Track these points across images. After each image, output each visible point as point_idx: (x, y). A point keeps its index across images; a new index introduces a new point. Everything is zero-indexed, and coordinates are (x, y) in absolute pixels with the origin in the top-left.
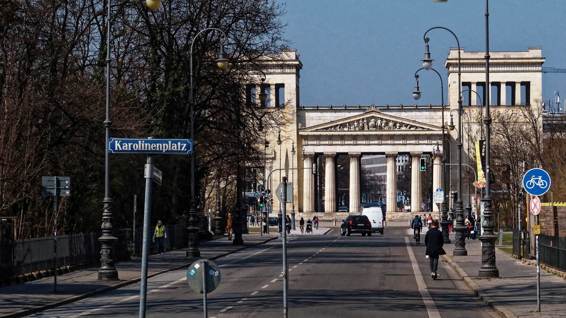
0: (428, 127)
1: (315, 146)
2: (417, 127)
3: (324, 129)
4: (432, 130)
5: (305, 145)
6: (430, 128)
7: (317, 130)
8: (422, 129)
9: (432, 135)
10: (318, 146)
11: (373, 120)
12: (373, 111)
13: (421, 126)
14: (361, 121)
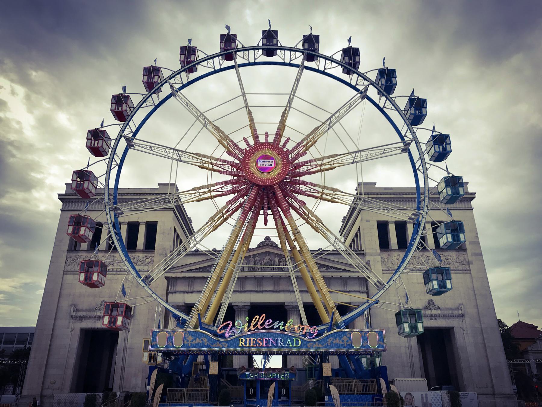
0: (343, 268)
1: (186, 295)
2: (328, 267)
3: (200, 268)
4: (349, 271)
5: (172, 293)
6: (347, 268)
7: (190, 271)
8: (335, 270)
9: (350, 277)
10: (190, 295)
11: (268, 257)
12: (267, 245)
13: (333, 265)
14: (252, 259)
